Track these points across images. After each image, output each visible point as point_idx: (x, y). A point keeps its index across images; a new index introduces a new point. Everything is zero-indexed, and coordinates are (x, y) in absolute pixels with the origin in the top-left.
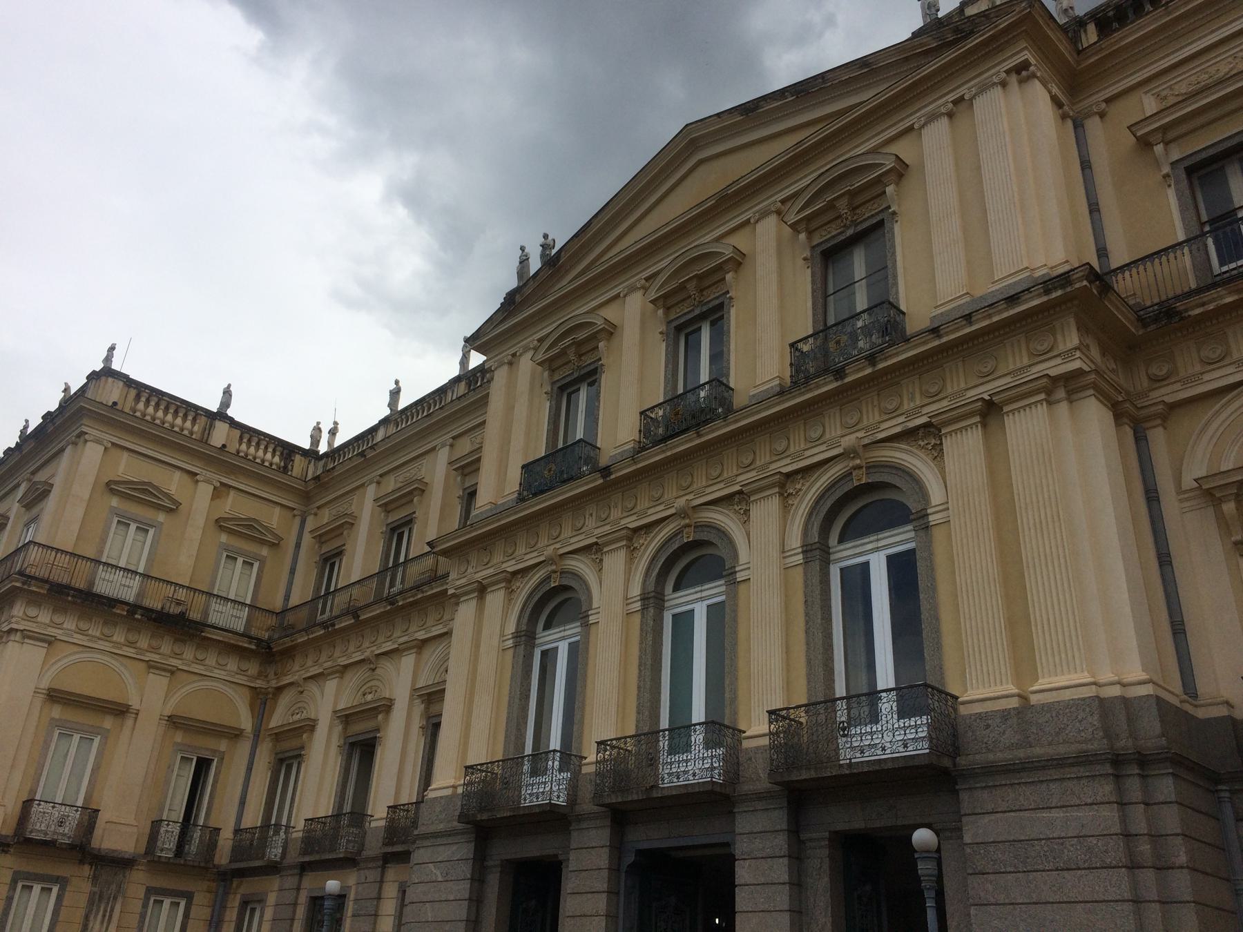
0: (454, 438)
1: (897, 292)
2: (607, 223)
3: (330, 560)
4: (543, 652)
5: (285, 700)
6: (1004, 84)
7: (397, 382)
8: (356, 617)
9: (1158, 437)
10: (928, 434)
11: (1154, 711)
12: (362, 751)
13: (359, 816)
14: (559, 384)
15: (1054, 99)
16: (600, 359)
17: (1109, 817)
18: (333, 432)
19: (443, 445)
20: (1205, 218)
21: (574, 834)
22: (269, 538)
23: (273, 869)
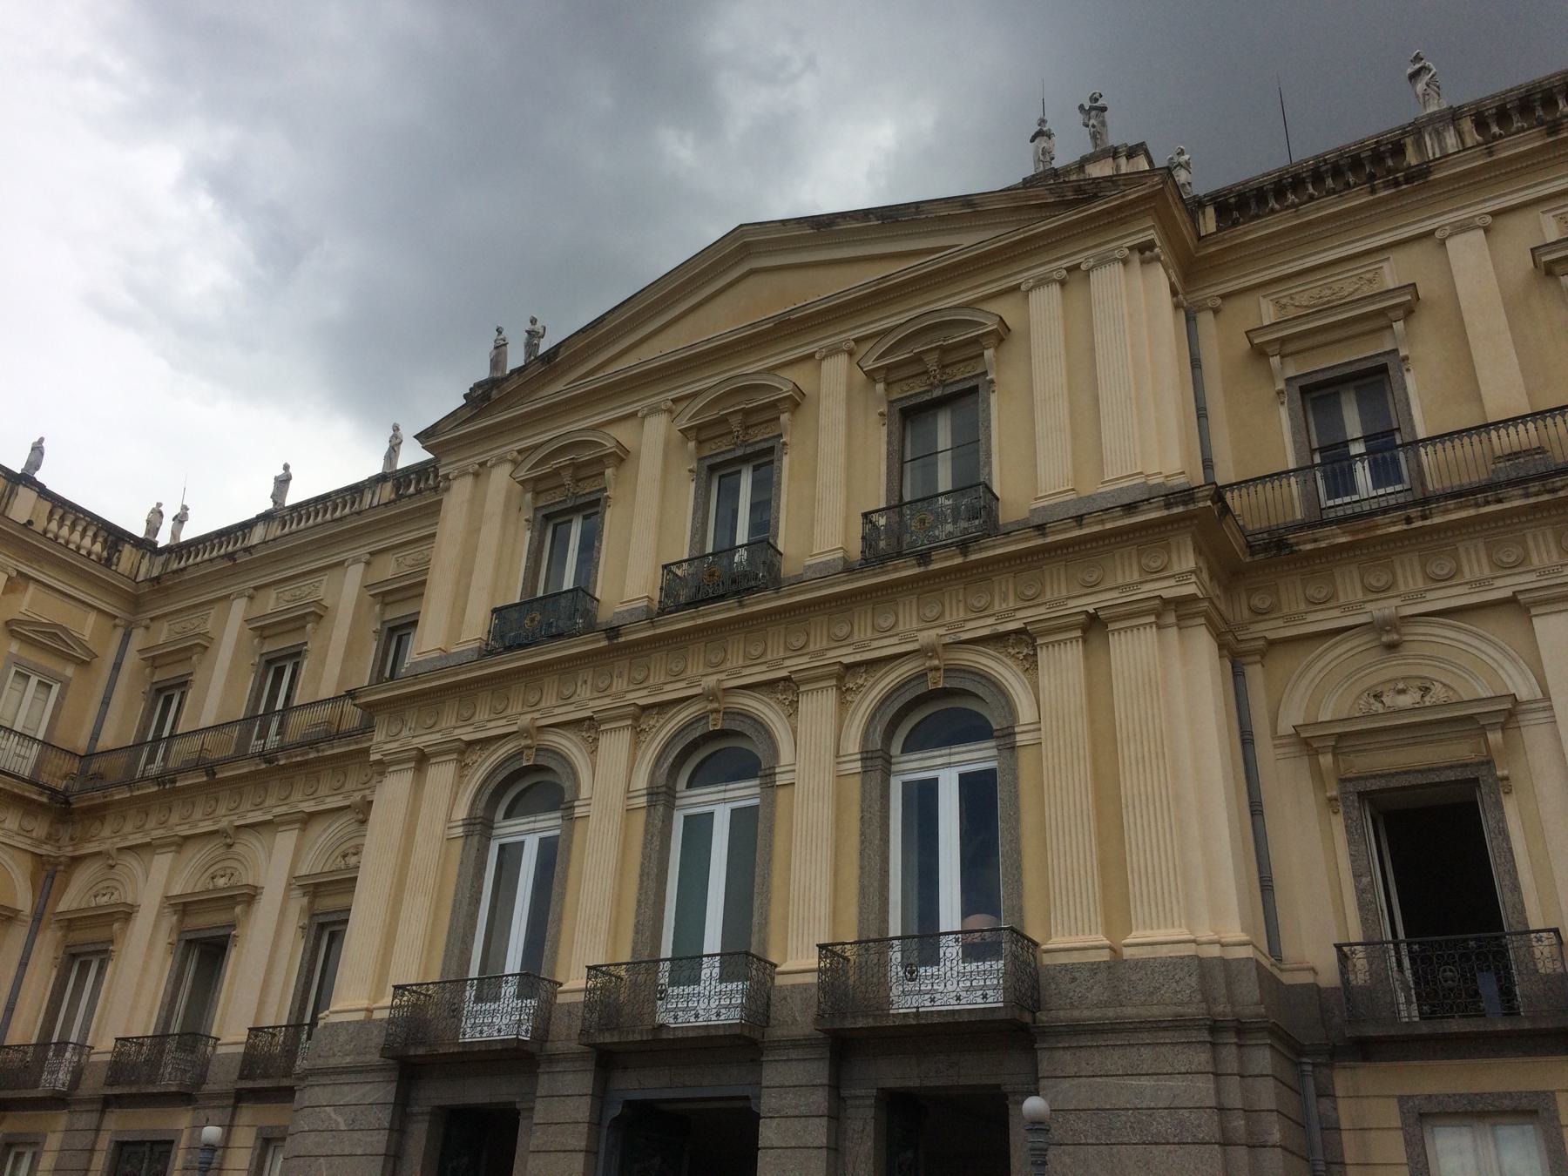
0: (372, 554)
1: (990, 473)
2: (623, 323)
3: (167, 693)
4: (502, 847)
5: (84, 877)
6: (1125, 262)
7: (286, 467)
8: (211, 772)
10: (1022, 643)
11: (1254, 973)
12: (205, 954)
14: (545, 512)
15: (1172, 286)
16: (605, 489)
17: (1204, 1085)
18: (180, 519)
19: (356, 561)
20: (1315, 445)
21: (543, 1079)
22: (79, 653)
23: (58, 1101)
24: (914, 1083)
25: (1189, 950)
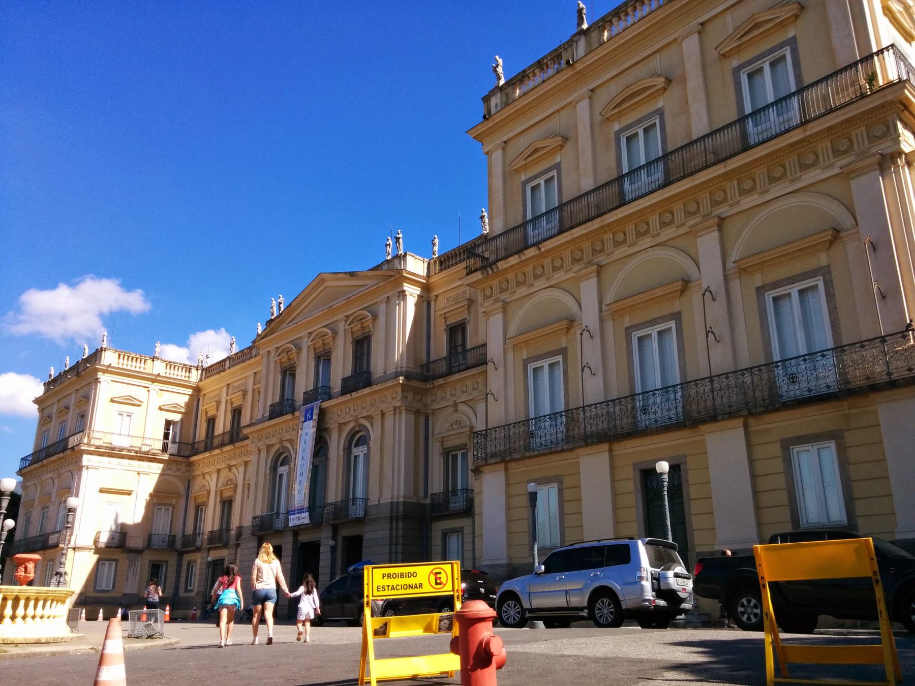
9: (430, 418)
12: (227, 504)
13: (228, 530)
23: (199, 549)
25: (390, 501)
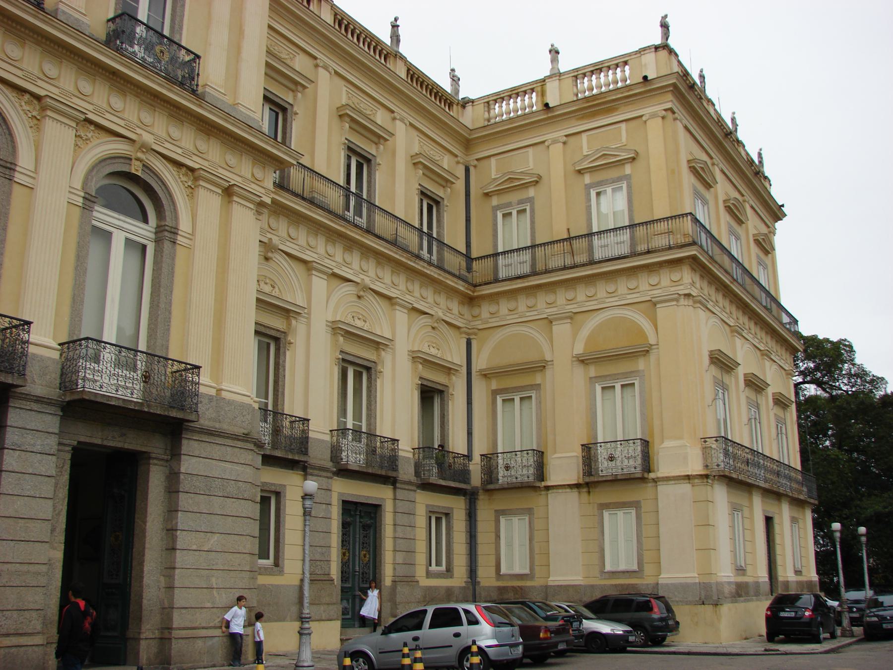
24: (98, 441)
